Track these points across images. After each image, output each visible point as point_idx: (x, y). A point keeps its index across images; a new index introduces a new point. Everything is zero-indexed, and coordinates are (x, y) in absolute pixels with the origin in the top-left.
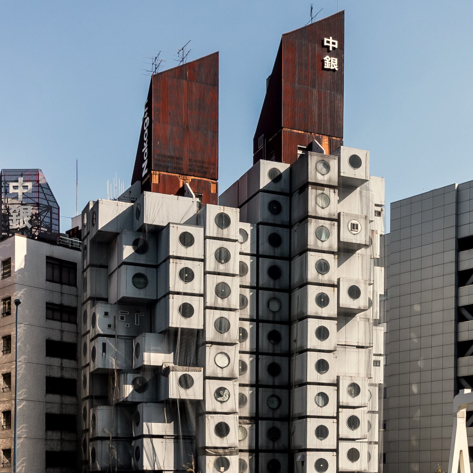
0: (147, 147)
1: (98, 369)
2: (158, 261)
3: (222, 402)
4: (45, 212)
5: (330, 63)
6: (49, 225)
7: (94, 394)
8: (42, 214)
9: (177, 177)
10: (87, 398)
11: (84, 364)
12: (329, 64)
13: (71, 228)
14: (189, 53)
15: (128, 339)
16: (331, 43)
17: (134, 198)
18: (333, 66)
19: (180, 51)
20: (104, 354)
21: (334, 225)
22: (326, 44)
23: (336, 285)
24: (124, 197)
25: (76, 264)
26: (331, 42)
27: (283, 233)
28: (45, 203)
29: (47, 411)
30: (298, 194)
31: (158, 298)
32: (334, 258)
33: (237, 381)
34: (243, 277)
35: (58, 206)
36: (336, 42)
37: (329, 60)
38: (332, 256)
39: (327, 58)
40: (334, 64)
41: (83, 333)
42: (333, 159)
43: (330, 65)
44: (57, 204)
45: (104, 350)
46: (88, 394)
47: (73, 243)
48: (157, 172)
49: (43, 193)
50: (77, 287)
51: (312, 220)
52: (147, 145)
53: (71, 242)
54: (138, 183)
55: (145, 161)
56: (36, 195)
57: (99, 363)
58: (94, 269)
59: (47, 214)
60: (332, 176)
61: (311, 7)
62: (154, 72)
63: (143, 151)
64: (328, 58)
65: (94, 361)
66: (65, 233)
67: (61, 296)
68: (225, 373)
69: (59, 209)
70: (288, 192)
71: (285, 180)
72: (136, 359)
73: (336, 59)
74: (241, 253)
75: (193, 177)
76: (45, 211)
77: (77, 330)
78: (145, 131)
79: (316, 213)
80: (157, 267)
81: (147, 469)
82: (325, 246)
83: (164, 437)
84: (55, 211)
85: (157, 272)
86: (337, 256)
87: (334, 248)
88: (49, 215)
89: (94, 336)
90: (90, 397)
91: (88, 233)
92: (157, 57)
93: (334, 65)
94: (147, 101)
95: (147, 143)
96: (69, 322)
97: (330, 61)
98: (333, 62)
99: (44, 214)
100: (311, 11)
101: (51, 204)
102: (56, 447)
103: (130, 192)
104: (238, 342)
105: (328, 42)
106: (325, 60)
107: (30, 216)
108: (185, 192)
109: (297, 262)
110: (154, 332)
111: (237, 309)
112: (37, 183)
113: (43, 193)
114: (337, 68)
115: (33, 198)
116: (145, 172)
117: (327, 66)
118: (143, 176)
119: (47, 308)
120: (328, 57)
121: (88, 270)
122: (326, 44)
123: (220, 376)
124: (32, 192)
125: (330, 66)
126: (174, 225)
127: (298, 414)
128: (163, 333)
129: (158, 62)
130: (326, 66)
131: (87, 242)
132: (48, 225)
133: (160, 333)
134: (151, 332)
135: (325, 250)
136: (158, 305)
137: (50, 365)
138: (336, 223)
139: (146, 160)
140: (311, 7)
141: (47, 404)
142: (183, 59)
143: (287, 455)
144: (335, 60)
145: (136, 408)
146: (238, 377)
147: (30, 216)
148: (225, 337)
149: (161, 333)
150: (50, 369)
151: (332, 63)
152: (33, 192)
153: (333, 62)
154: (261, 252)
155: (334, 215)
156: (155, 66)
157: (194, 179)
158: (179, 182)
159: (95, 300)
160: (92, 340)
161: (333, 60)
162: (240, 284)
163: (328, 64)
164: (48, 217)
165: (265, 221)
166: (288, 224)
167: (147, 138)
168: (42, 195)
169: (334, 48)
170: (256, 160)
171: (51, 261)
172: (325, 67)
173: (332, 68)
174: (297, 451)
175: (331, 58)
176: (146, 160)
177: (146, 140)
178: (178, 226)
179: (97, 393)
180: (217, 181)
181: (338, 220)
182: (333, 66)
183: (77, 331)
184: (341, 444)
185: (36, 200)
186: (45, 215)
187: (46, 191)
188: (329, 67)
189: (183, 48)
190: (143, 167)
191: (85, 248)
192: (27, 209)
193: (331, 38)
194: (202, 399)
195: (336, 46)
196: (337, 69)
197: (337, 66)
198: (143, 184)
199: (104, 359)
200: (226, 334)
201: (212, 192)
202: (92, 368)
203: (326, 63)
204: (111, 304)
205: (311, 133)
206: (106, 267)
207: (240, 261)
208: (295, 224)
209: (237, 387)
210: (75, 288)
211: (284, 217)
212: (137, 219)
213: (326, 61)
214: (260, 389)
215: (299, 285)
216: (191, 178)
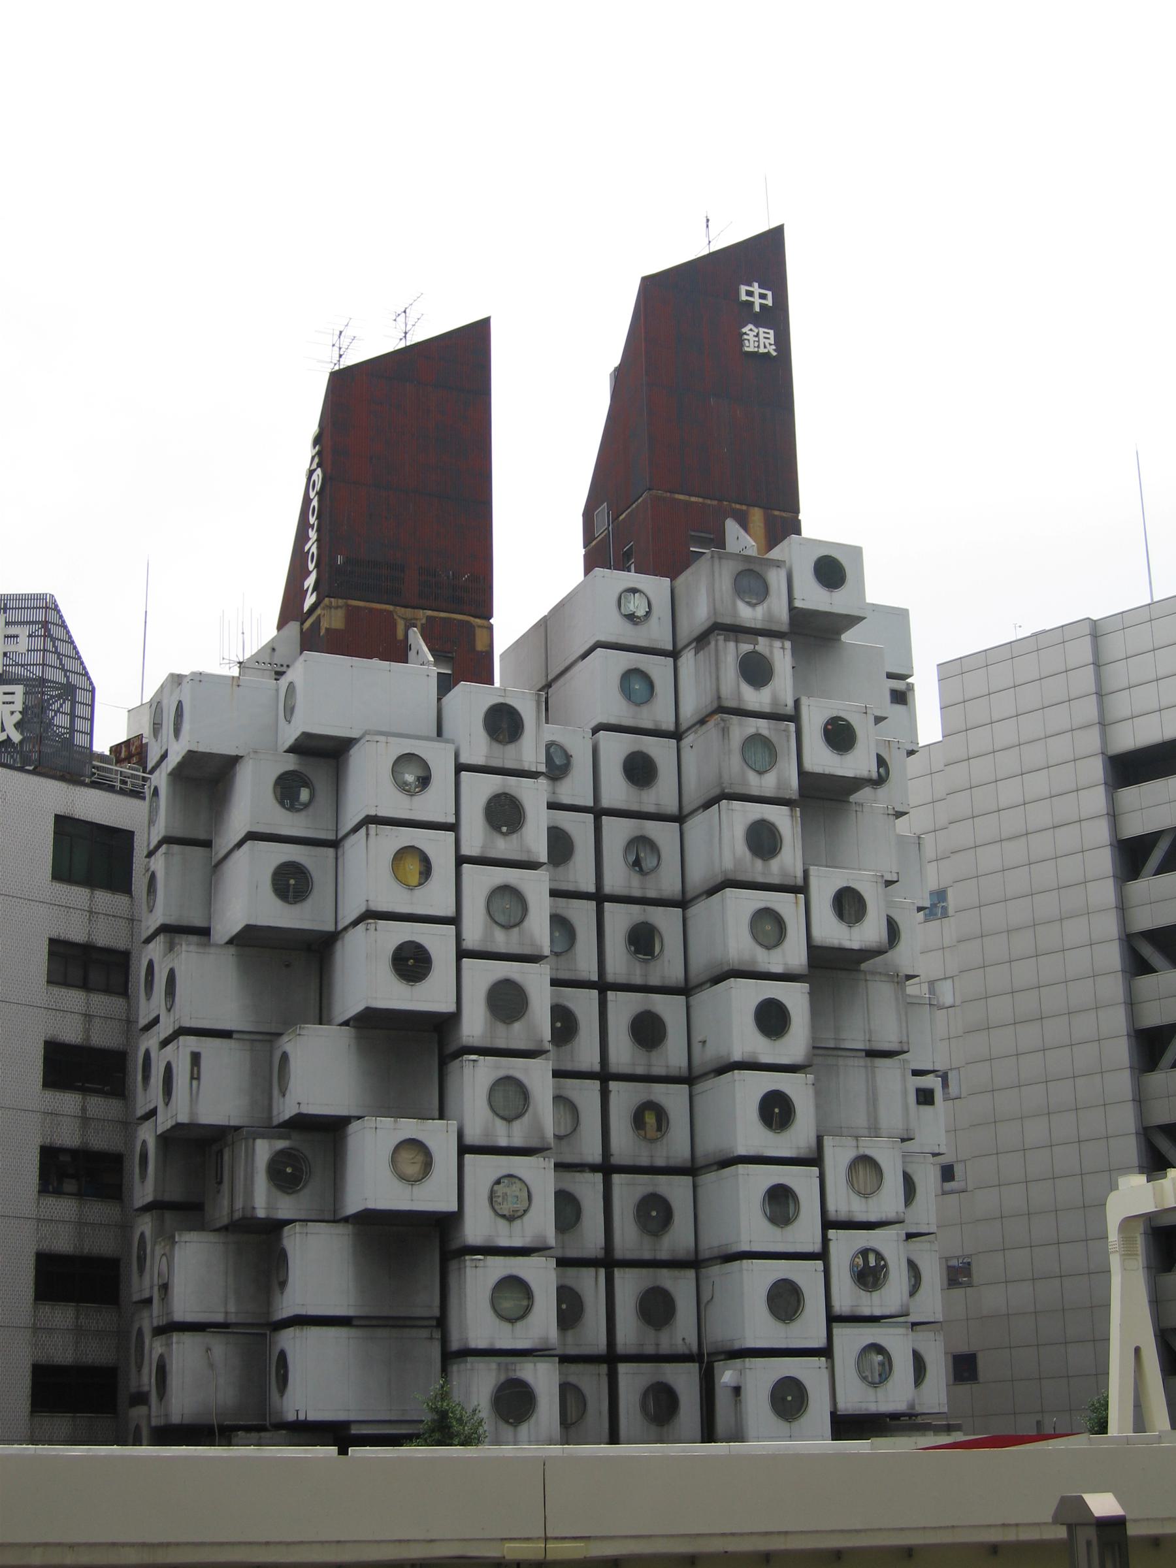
0: (316, 540)
1: (178, 1126)
2: (339, 827)
3: (510, 1218)
4: (56, 701)
5: (757, 339)
6: (67, 733)
7: (167, 1197)
8: (51, 705)
9: (390, 613)
10: (147, 1208)
11: (140, 1112)
12: (754, 341)
13: (125, 739)
14: (419, 321)
15: (259, 1041)
16: (756, 295)
17: (282, 666)
18: (765, 347)
19: (399, 315)
20: (195, 1083)
21: (786, 730)
22: (744, 297)
23: (801, 887)
24: (257, 662)
25: (132, 833)
26: (755, 295)
27: (660, 751)
28: (59, 677)
29: (39, 1245)
30: (693, 652)
31: (340, 927)
32: (792, 816)
33: (549, 1158)
34: (561, 869)
35: (91, 683)
36: (769, 294)
37: (755, 334)
38: (785, 809)
39: (749, 330)
40: (767, 342)
41: (143, 1022)
42: (775, 568)
43: (756, 344)
44: (89, 678)
45: (195, 1076)
46: (149, 1198)
47: (127, 779)
48: (340, 601)
49: (56, 652)
50: (131, 897)
51: (731, 718)
52: (316, 535)
53: (121, 776)
54: (293, 627)
55: (312, 572)
56: (37, 657)
57: (180, 1111)
58: (176, 848)
59: (61, 706)
60: (776, 609)
61: (707, 217)
62: (335, 364)
63: (306, 551)
64: (751, 330)
65: (167, 1104)
66: (107, 753)
67: (90, 920)
68: (517, 1135)
69: (93, 691)
70: (670, 647)
71: (659, 619)
72: (281, 1100)
73: (772, 332)
74: (552, 806)
75: (429, 613)
76: (59, 697)
77: (128, 1014)
78: (312, 500)
79: (739, 700)
80: (335, 844)
81: (308, 1419)
82: (767, 784)
83: (355, 1323)
84: (80, 696)
85: (337, 859)
86: (798, 809)
87: (791, 790)
88: (67, 707)
89: (170, 1031)
90: (154, 1207)
91: (164, 756)
92: (342, 330)
93: (767, 345)
94: (318, 432)
95: (317, 531)
96: (108, 990)
97: (757, 335)
98: (765, 338)
99: (55, 707)
100: (707, 226)
101: (75, 680)
102: (62, 1353)
103: (274, 649)
104: (548, 1046)
105: (749, 293)
106: (745, 333)
107: (20, 712)
108: (410, 649)
109: (697, 826)
110: (329, 1023)
111: (547, 957)
112: (41, 629)
113: (56, 652)
114: (775, 350)
115: (30, 665)
116: (310, 600)
117: (750, 347)
118: (305, 610)
119: (51, 954)
120: (750, 326)
121: (164, 848)
122: (744, 297)
123: (503, 1142)
124: (28, 650)
125: (758, 347)
126: (382, 739)
127: (718, 1247)
128: (351, 1023)
129: (345, 342)
130: (749, 347)
131: (160, 779)
132: (63, 734)
133: (341, 1025)
134: (321, 1023)
135: (768, 795)
136: (339, 945)
137: (51, 1113)
138: (792, 726)
139: (313, 570)
140: (707, 217)
141: (42, 1226)
142: (406, 333)
143: (694, 1367)
144: (768, 333)
145: (279, 1239)
146: (552, 1145)
147: (20, 712)
148: (515, 1035)
149: (346, 1023)
150: (51, 1123)
151: (762, 340)
152: (31, 650)
153: (765, 338)
154: (606, 803)
155: (786, 706)
156: (338, 349)
157: (435, 618)
158: (394, 626)
159: (174, 932)
160: (165, 1043)
161: (765, 332)
162: (552, 887)
163: (752, 342)
164: (67, 714)
165: (613, 720)
166: (672, 727)
167: (317, 518)
168: (52, 659)
169: (761, 305)
170: (588, 571)
171: (64, 825)
172: (747, 349)
173: (762, 350)
174: (722, 1357)
175: (757, 327)
176: (313, 570)
177: (314, 524)
178: (391, 739)
179: (174, 1194)
180: (492, 621)
181: (795, 718)
182: (765, 347)
183: (128, 1017)
184: (839, 1331)
185: (38, 671)
186: (58, 709)
187: (63, 648)
188: (756, 350)
189: (406, 308)
190: (305, 588)
191: (156, 792)
192: (13, 693)
193: (756, 285)
194: (454, 1207)
195: (769, 302)
196: (774, 354)
197: (774, 347)
198: (304, 630)
199: (194, 1098)
200: (517, 1026)
201: (480, 646)
202: (164, 1122)
203: (749, 340)
204: (217, 945)
205: (720, 500)
206: (207, 844)
207: (551, 825)
208: (689, 729)
209: (551, 1173)
210: (127, 898)
211: (661, 713)
212: (287, 721)
213: (748, 335)
214: (616, 1178)
215: (706, 887)
216: (422, 615)
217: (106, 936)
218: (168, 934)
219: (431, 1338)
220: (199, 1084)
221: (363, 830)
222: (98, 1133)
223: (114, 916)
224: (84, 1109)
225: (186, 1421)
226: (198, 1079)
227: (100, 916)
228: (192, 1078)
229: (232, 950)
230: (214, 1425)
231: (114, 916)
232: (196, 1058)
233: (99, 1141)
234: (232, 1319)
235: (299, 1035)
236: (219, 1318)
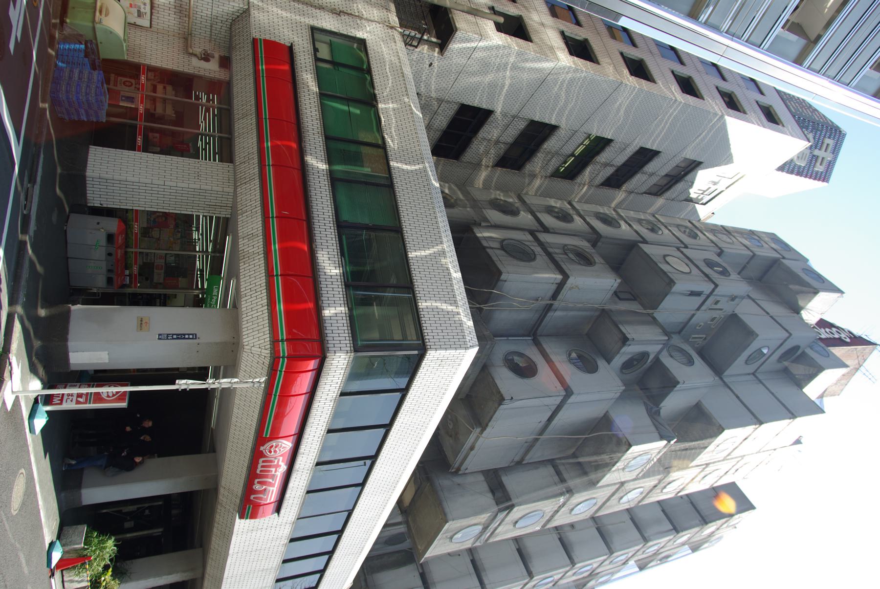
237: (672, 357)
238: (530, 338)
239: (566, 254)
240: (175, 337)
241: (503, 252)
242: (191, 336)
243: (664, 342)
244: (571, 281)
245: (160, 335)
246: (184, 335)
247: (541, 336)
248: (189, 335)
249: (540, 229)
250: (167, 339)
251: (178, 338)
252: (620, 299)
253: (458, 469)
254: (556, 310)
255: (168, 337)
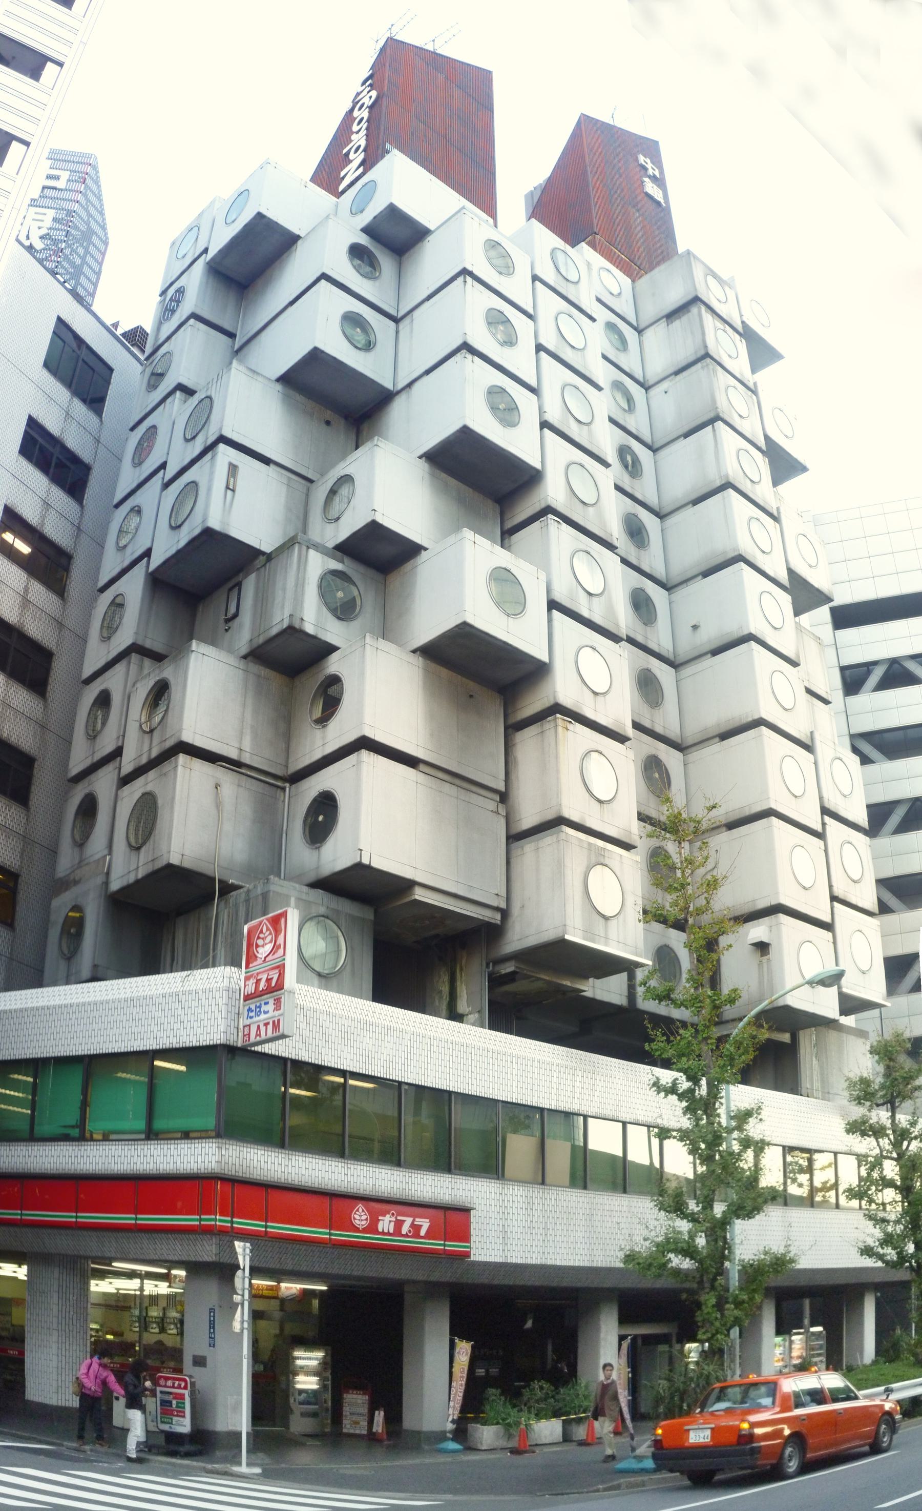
217: (75, 441)
218: (184, 394)
219: (497, 813)
220: (233, 497)
221: (460, 279)
222: (35, 620)
223: (84, 428)
224: (26, 590)
225: (187, 864)
226: (233, 491)
227: (74, 421)
228: (227, 488)
229: (279, 387)
230: (214, 879)
231: (84, 428)
232: (233, 469)
233: (36, 629)
234: (246, 759)
235: (377, 445)
236: (233, 754)
237: (338, 518)
238: (287, 790)
239: (152, 731)
240: (212, 1330)
241: (143, 850)
242: (212, 1314)
243: (304, 548)
244: (188, 737)
245: (210, 1346)
246: (210, 1321)
247: (287, 767)
248: (210, 1316)
249: (115, 763)
250: (214, 1338)
251: (214, 1328)
252: (236, 615)
253: (497, 909)
254: (241, 750)
255: (212, 1338)
